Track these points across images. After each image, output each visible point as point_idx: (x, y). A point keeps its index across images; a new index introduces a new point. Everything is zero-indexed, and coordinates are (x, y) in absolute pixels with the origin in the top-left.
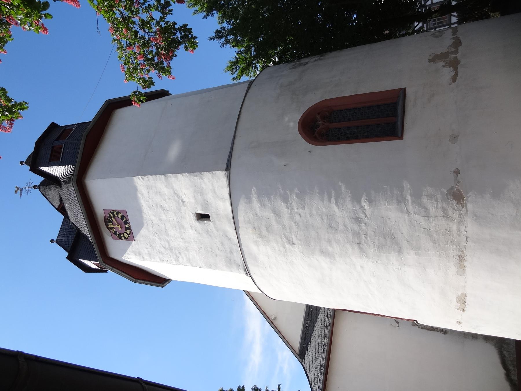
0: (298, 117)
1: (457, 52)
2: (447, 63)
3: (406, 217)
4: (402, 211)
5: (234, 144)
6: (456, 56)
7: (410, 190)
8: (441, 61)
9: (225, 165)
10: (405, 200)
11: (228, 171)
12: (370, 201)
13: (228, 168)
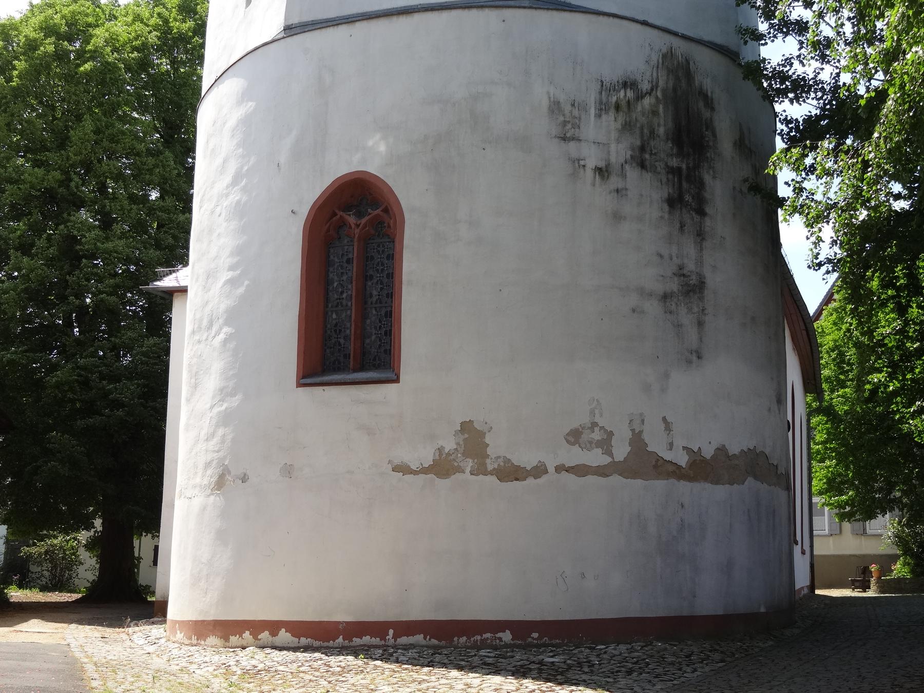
0: (373, 168)
1: (480, 470)
2: (449, 454)
3: (208, 406)
4: (213, 397)
5: (336, 27)
6: (468, 470)
7: (231, 408)
8: (458, 444)
9: (295, 20)
10: (222, 400)
11: (282, 35)
12: (225, 342)
13: (290, 30)
